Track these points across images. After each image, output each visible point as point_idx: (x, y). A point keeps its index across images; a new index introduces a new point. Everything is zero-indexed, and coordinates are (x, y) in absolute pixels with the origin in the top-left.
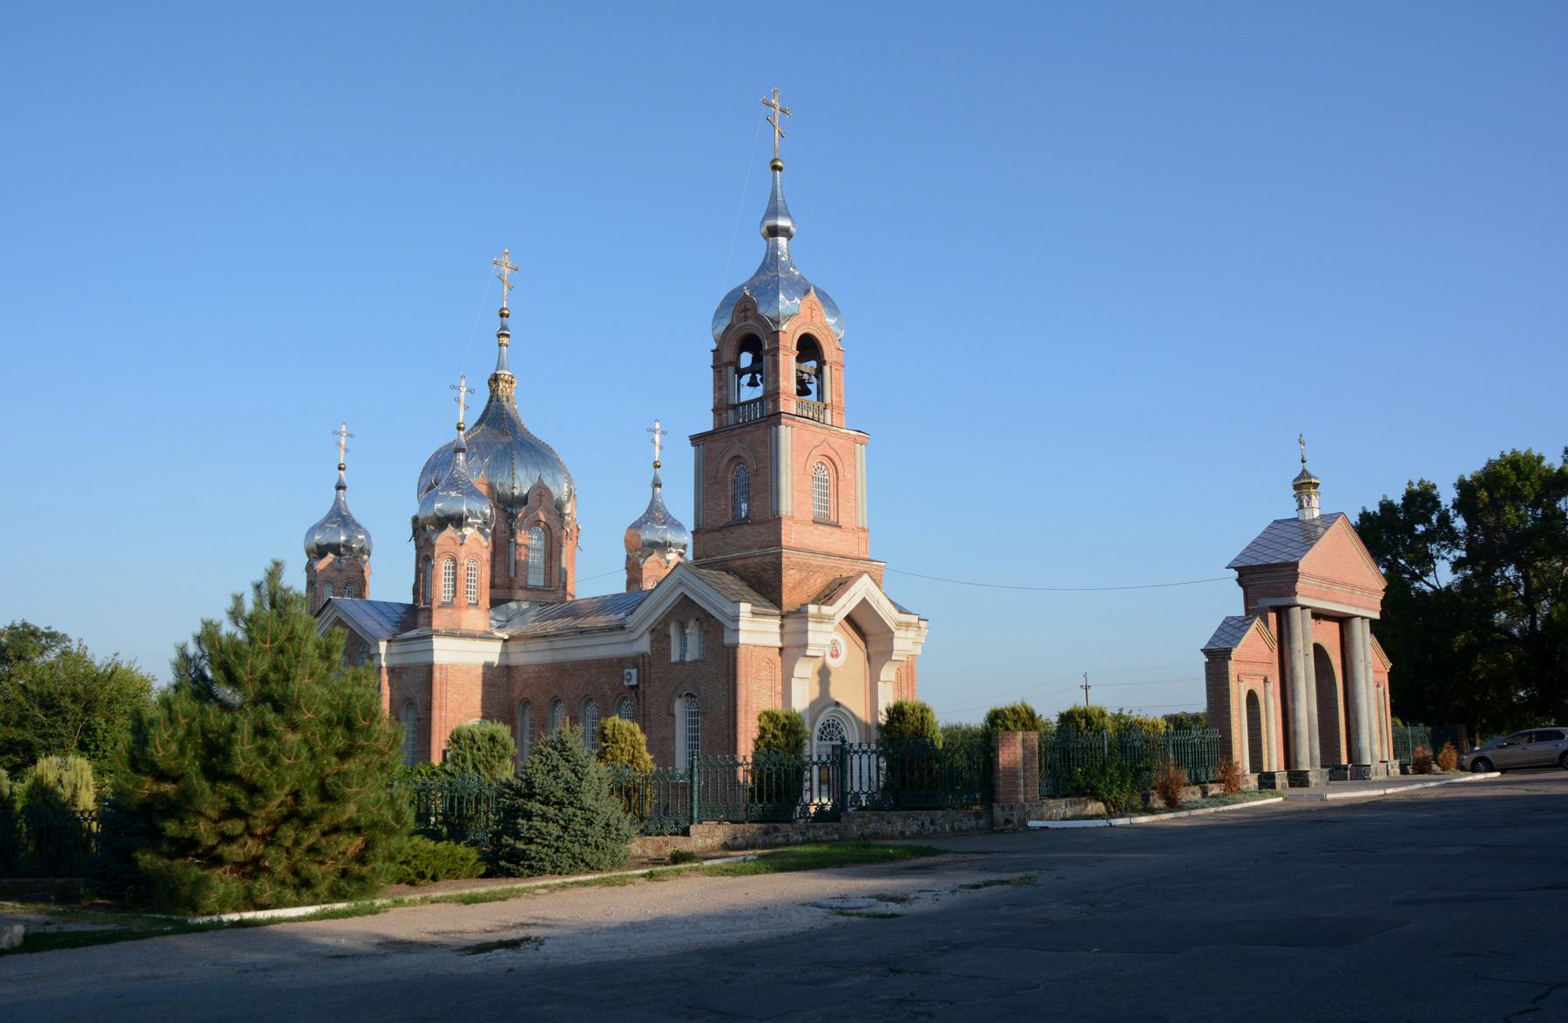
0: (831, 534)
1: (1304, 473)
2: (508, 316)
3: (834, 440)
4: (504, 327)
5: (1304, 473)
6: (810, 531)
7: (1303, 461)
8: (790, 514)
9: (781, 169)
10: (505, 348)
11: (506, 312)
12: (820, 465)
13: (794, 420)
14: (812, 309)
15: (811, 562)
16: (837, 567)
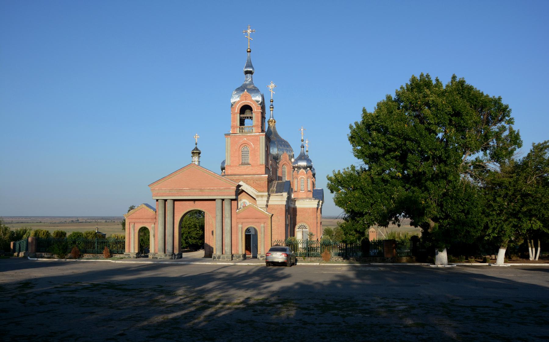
0: (247, 168)
1: (196, 149)
2: (273, 102)
3: (249, 138)
4: (272, 105)
5: (196, 149)
6: (238, 169)
7: (196, 144)
8: (229, 165)
9: (250, 52)
10: (272, 111)
11: (272, 100)
12: (244, 147)
13: (230, 135)
14: (246, 97)
15: (233, 178)
16: (245, 179)
